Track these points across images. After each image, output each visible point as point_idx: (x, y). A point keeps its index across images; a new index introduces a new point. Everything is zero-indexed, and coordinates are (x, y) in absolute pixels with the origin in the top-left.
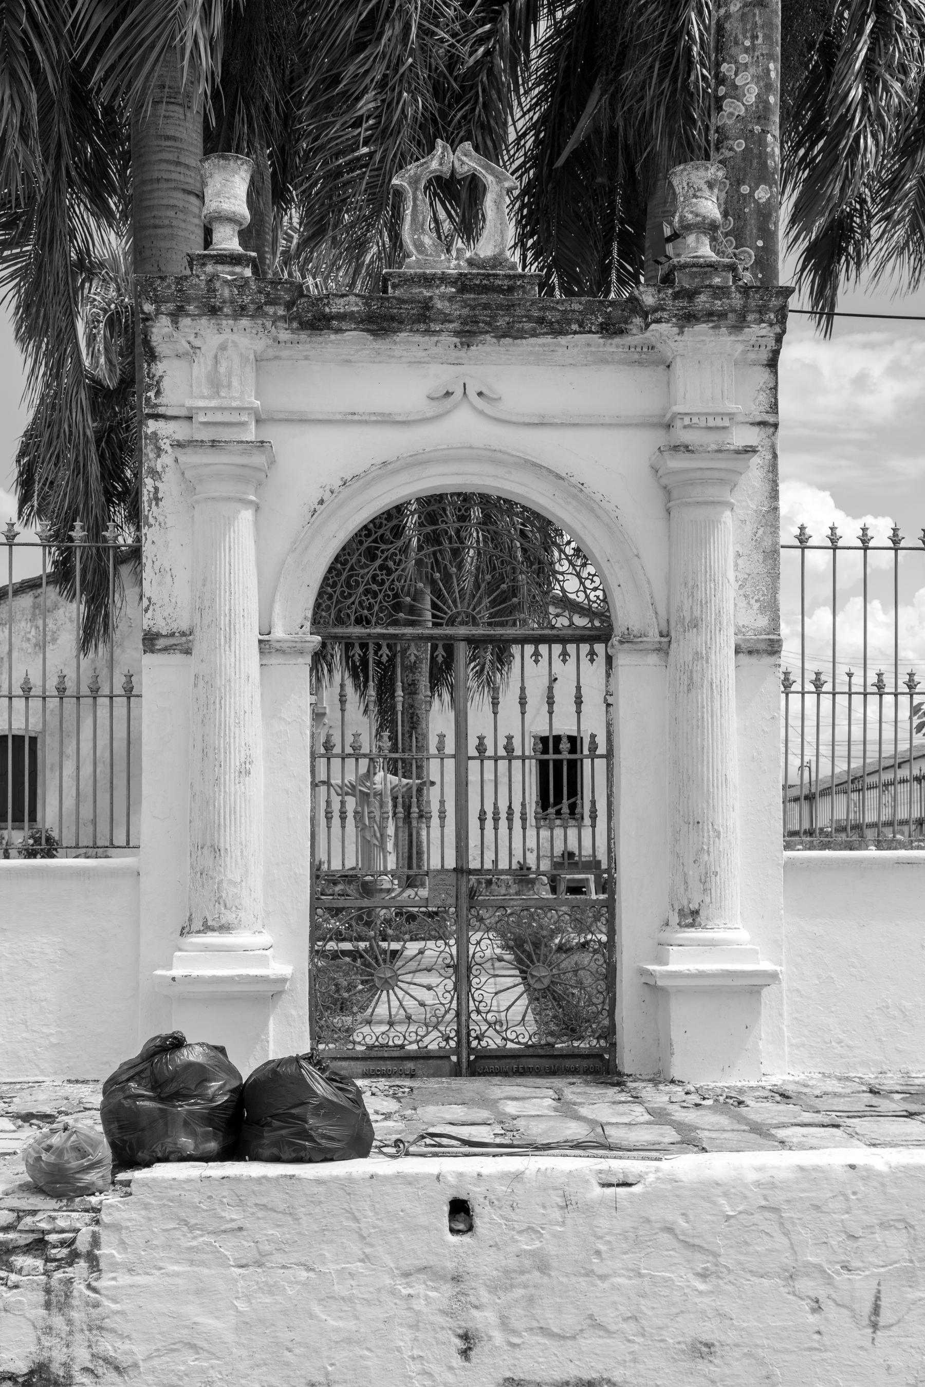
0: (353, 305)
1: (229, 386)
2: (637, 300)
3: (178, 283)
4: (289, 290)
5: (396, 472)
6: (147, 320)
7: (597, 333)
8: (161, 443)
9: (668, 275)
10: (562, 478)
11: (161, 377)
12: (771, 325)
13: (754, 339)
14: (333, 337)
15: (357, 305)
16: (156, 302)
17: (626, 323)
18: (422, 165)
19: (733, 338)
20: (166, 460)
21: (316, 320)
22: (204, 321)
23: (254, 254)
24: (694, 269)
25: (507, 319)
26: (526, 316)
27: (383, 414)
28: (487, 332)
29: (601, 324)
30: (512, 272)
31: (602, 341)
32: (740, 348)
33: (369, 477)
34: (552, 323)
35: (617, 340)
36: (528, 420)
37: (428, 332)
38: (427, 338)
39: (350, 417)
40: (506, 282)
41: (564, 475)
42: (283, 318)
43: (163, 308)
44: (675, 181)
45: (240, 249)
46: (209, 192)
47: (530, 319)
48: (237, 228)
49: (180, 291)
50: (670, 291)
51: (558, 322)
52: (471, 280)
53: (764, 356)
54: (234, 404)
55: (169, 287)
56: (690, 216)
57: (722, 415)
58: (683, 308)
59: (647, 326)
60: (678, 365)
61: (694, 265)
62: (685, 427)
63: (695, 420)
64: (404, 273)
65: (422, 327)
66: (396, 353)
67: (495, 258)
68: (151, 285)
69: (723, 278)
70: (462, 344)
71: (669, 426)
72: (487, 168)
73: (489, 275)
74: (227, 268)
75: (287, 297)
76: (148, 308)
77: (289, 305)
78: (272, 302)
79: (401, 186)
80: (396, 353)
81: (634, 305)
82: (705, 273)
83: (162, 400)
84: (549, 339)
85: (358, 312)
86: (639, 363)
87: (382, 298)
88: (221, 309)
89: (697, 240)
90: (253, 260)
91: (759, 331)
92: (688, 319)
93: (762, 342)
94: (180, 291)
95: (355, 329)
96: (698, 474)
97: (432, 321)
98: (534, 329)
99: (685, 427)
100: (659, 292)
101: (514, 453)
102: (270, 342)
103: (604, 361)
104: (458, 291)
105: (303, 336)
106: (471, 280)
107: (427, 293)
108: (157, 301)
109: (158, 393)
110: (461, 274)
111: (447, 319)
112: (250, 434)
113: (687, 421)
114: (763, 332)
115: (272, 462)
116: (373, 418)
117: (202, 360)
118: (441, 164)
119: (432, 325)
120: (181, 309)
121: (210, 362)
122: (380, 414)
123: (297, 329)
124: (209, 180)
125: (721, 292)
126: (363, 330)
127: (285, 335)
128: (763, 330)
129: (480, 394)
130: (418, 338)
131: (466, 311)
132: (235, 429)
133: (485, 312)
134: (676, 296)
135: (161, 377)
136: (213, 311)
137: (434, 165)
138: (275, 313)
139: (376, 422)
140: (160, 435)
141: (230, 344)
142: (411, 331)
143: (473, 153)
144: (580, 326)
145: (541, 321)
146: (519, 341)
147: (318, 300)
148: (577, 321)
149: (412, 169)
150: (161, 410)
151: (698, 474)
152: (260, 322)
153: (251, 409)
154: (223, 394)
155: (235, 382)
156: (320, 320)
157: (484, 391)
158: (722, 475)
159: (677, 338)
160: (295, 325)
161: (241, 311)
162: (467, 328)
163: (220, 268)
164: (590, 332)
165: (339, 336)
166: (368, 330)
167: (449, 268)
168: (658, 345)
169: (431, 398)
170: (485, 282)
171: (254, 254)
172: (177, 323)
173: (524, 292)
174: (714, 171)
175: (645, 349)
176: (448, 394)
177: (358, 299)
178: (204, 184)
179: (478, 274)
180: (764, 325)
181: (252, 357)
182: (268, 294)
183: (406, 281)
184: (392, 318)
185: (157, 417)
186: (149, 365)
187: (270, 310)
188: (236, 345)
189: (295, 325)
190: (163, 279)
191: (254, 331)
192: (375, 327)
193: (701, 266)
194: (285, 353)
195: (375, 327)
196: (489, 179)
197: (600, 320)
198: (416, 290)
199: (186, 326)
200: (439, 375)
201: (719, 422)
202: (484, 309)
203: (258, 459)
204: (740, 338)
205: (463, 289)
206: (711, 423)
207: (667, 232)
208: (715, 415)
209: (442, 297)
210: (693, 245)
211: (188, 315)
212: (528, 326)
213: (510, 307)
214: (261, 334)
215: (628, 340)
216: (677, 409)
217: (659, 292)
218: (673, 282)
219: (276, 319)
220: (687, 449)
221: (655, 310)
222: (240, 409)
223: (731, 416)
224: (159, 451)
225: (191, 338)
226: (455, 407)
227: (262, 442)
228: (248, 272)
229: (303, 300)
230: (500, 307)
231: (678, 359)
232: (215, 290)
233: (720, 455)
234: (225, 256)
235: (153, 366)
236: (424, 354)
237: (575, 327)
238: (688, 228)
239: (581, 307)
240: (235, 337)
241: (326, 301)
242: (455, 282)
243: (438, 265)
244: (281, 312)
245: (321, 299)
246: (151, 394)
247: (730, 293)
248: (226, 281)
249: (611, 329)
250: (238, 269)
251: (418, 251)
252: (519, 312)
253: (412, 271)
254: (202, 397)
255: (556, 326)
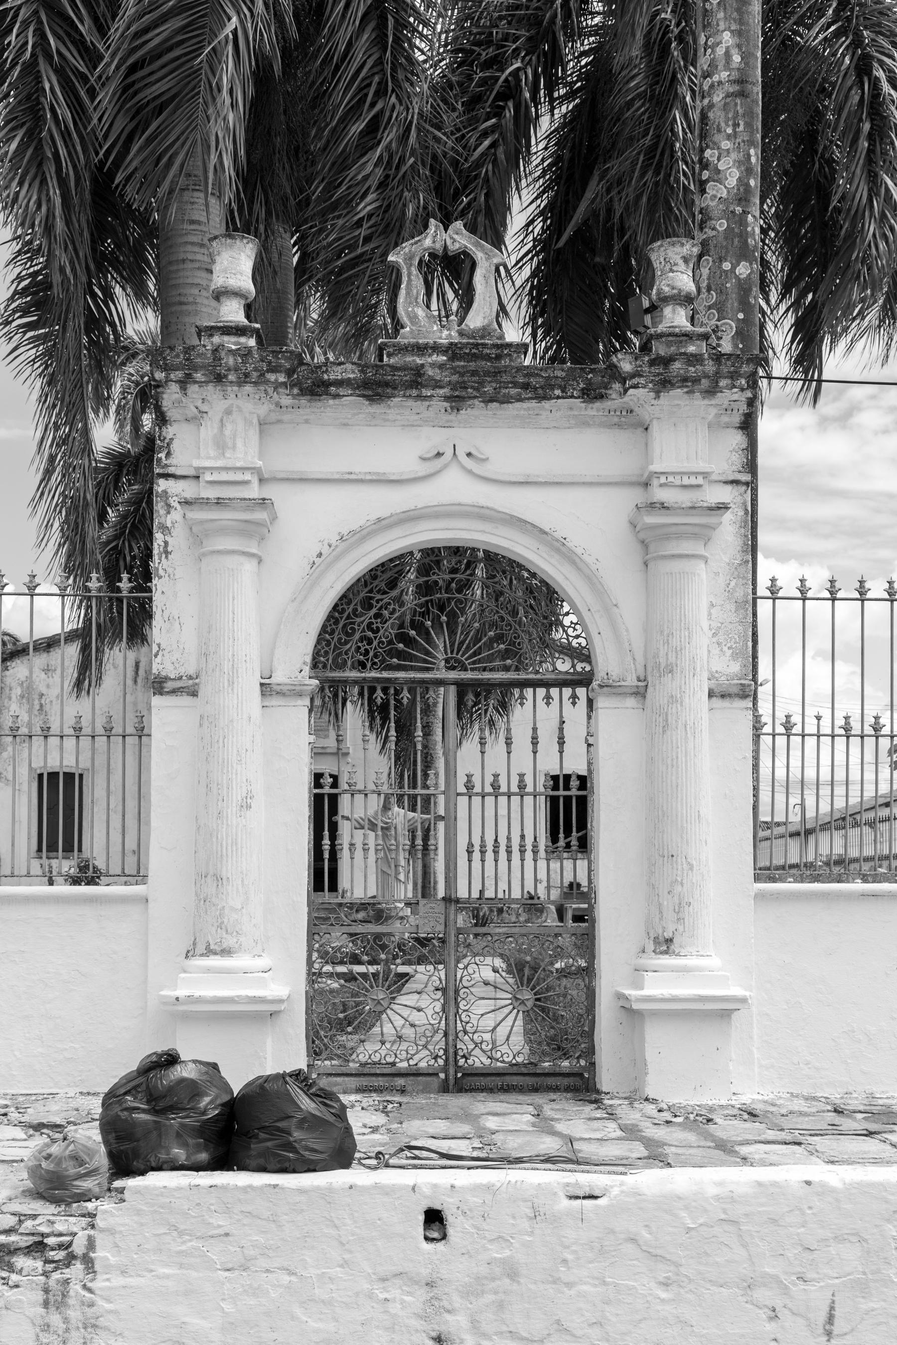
0: (350, 372)
1: (234, 447)
2: (616, 367)
3: (186, 353)
4: (290, 358)
5: (390, 526)
6: (158, 386)
7: (578, 397)
8: (171, 501)
9: (646, 344)
10: (545, 533)
11: (172, 439)
12: (742, 390)
13: (726, 403)
14: (331, 402)
15: (353, 372)
16: (166, 370)
17: (606, 388)
18: (416, 243)
19: (706, 402)
20: (176, 515)
21: (315, 387)
22: (210, 387)
23: (258, 326)
24: (671, 338)
25: (494, 385)
26: (512, 382)
27: (378, 474)
28: (475, 397)
29: (583, 389)
30: (499, 342)
31: (583, 405)
32: (713, 411)
33: (365, 532)
34: (536, 389)
35: (598, 404)
36: (514, 479)
37: (420, 397)
38: (419, 403)
39: (347, 477)
40: (494, 351)
41: (547, 530)
42: (284, 384)
43: (172, 376)
44: (653, 257)
45: (246, 321)
46: (217, 268)
47: (515, 385)
48: (243, 302)
49: (187, 360)
50: (647, 359)
51: (542, 387)
52: (461, 349)
53: (737, 419)
54: (238, 465)
55: (177, 356)
56: (666, 289)
57: (696, 474)
58: (659, 374)
59: (626, 391)
60: (655, 428)
61: (670, 335)
62: (661, 485)
63: (671, 479)
64: (399, 343)
65: (415, 392)
66: (390, 417)
67: (484, 328)
68: (161, 354)
69: (698, 346)
70: (452, 408)
71: (646, 485)
72: (477, 245)
73: (477, 345)
74: (233, 339)
75: (288, 365)
76: (159, 375)
77: (290, 373)
78: (273, 370)
79: (397, 262)
80: (390, 417)
81: (614, 373)
82: (681, 342)
83: (172, 461)
84: (533, 404)
85: (354, 379)
86: (619, 426)
87: (376, 366)
88: (226, 376)
89: (674, 310)
90: (257, 331)
91: (733, 397)
92: (663, 384)
93: (735, 406)
94: (187, 360)
95: (351, 395)
96: (673, 529)
97: (424, 386)
98: (519, 394)
99: (661, 485)
100: (636, 359)
101: (500, 509)
102: (273, 407)
103: (585, 424)
104: (449, 360)
105: (304, 401)
106: (461, 349)
107: (419, 361)
108: (167, 368)
109: (168, 455)
110: (451, 344)
111: (438, 385)
112: (254, 491)
113: (663, 480)
114: (735, 397)
115: (274, 518)
116: (368, 477)
117: (209, 423)
118: (434, 242)
119: (424, 390)
120: (188, 376)
121: (216, 425)
122: (375, 473)
123: (298, 395)
124: (217, 258)
125: (694, 359)
126: (359, 396)
127: (286, 401)
128: (736, 394)
129: (469, 455)
130: (410, 403)
131: (455, 378)
132: (240, 488)
133: (474, 379)
134: (652, 363)
135: (172, 439)
136: (219, 379)
137: (428, 242)
138: (276, 380)
139: (371, 481)
140: (170, 493)
141: (234, 409)
142: (404, 396)
143: (464, 231)
144: (563, 392)
145: (526, 386)
146: (505, 405)
147: (317, 367)
148: (560, 387)
149: (407, 247)
150: (171, 470)
151: (673, 529)
152: (262, 388)
153: (254, 468)
154: (227, 455)
155: (239, 443)
156: (319, 386)
157: (474, 452)
158: (696, 530)
159: (653, 402)
160: (296, 391)
161: (244, 379)
162: (457, 393)
163: (226, 338)
164: (572, 397)
165: (337, 401)
166: (363, 396)
167: (441, 338)
168: (636, 409)
169: (424, 459)
170: (474, 351)
171: (258, 326)
172: (185, 389)
173: (511, 360)
174: (690, 248)
175: (624, 413)
176: (439, 455)
177: (354, 367)
178: (213, 262)
179: (468, 343)
180: (735, 390)
181: (255, 421)
182: (270, 362)
183: (400, 350)
184: (387, 384)
185: (167, 476)
186: (160, 428)
187: (272, 377)
188: (240, 410)
189: (296, 391)
190: (172, 349)
191: (257, 397)
192: (370, 393)
193: (676, 335)
194: (286, 417)
195: (370, 393)
196: (479, 256)
197: (582, 385)
198: (409, 359)
199: (193, 392)
200: (432, 438)
201: (693, 481)
202: (472, 375)
203: (260, 515)
204: (713, 402)
205: (454, 357)
206: (686, 481)
207: (646, 304)
208: (689, 474)
209: (433, 365)
210: (670, 315)
211: (196, 382)
212: (514, 391)
213: (497, 373)
214: (263, 400)
215: (608, 404)
216: (655, 467)
217: (636, 359)
218: (650, 350)
219: (277, 386)
220: (663, 507)
221: (633, 376)
222: (243, 469)
223: (705, 475)
224: (169, 506)
225: (199, 403)
226: (446, 466)
227: (264, 499)
228: (252, 342)
229: (303, 368)
230: (487, 373)
231: (655, 422)
232: (220, 359)
233: (694, 512)
234: (231, 327)
235: (164, 429)
236: (417, 417)
237: (558, 392)
238: (665, 300)
239: (564, 374)
240: (239, 402)
241: (324, 369)
242: (446, 351)
243: (431, 335)
244: (282, 378)
245: (320, 367)
246: (162, 455)
247: (703, 360)
248: (231, 351)
249: (592, 394)
250: (243, 340)
251: (412, 323)
252: (505, 378)
253: (406, 341)
254: (209, 458)
255: (540, 391)
